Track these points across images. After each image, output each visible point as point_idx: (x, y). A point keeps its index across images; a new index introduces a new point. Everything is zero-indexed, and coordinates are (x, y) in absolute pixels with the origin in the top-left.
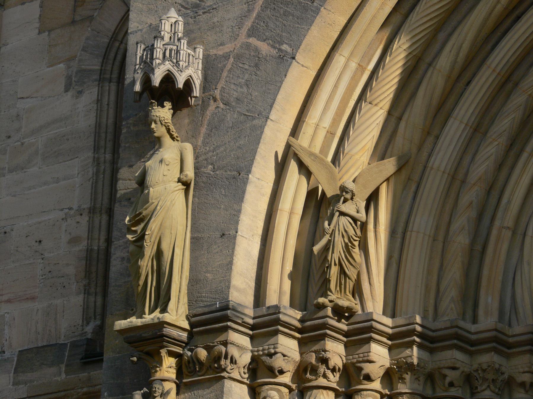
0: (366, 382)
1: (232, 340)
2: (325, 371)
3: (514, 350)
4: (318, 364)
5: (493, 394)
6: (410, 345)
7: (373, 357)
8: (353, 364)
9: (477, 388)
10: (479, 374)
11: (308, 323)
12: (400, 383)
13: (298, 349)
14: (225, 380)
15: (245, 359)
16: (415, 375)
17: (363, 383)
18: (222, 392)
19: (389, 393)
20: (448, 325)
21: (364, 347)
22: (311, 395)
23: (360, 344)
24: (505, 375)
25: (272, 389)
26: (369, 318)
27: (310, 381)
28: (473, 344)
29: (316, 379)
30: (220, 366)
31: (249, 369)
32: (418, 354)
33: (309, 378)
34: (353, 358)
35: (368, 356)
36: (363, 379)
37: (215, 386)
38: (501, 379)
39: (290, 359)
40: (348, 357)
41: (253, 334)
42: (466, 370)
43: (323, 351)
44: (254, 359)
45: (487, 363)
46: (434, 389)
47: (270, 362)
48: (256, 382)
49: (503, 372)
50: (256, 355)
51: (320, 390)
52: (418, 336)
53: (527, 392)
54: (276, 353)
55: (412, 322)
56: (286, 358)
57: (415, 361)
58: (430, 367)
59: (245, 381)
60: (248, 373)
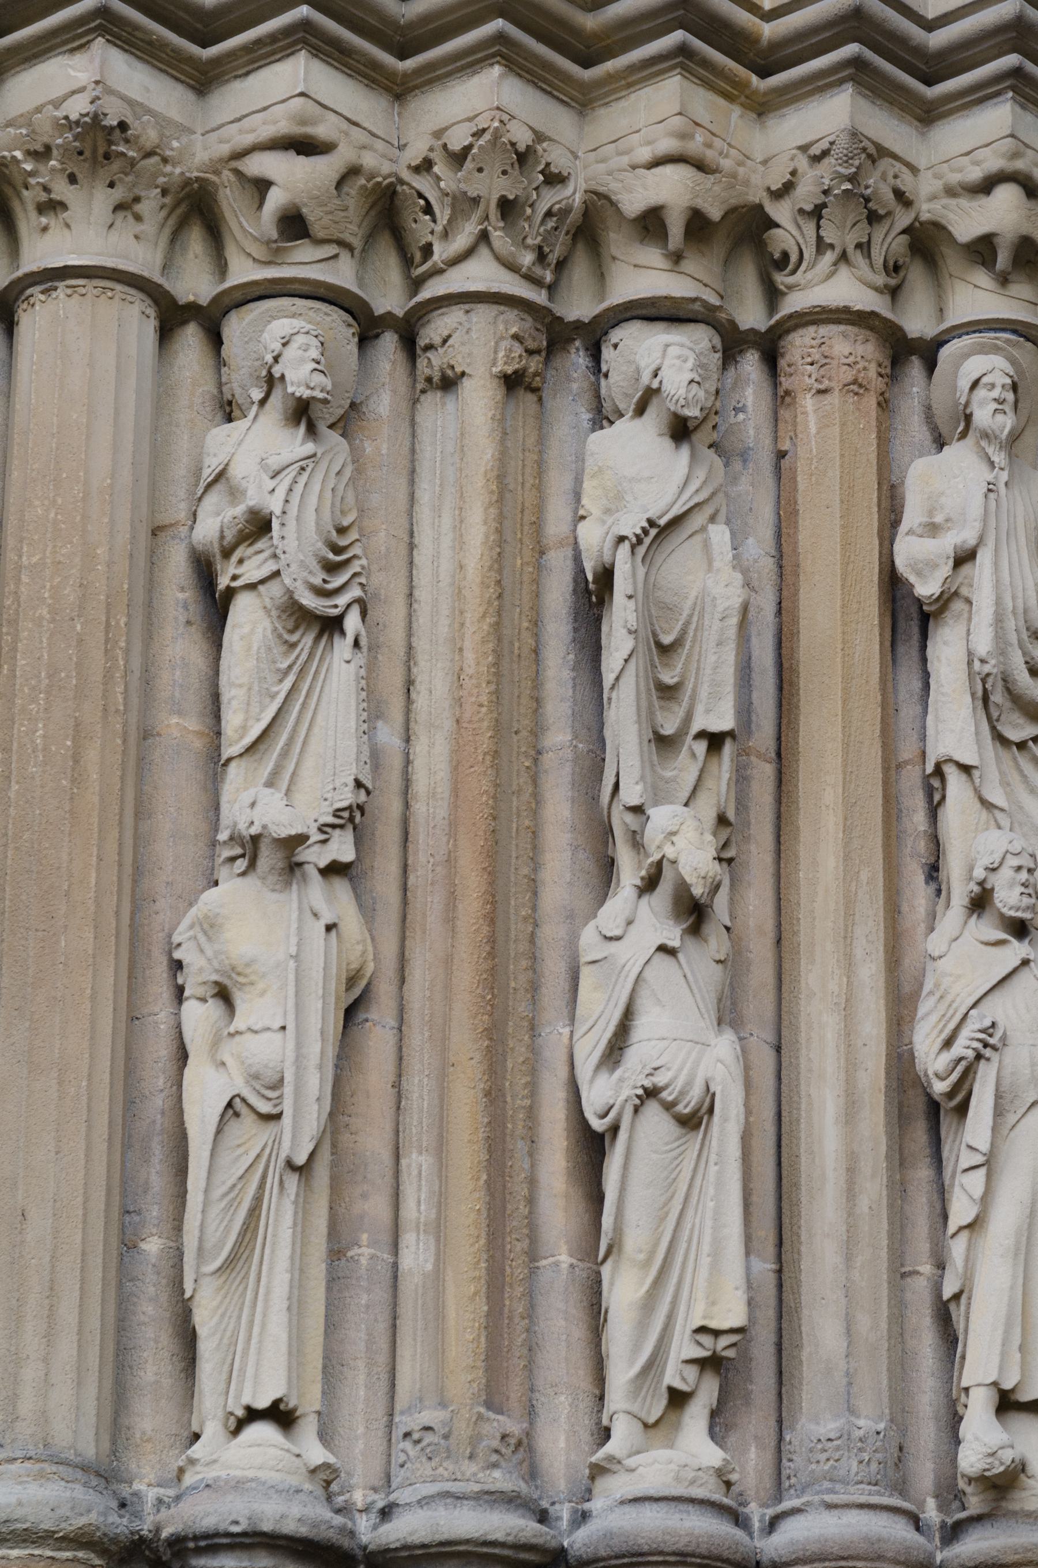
9: (427, 250)
16: (111, 185)
24: (569, 191)
38: (542, 208)
42: (368, 161)
45: (470, 119)
46: (222, 268)
49: (554, 169)
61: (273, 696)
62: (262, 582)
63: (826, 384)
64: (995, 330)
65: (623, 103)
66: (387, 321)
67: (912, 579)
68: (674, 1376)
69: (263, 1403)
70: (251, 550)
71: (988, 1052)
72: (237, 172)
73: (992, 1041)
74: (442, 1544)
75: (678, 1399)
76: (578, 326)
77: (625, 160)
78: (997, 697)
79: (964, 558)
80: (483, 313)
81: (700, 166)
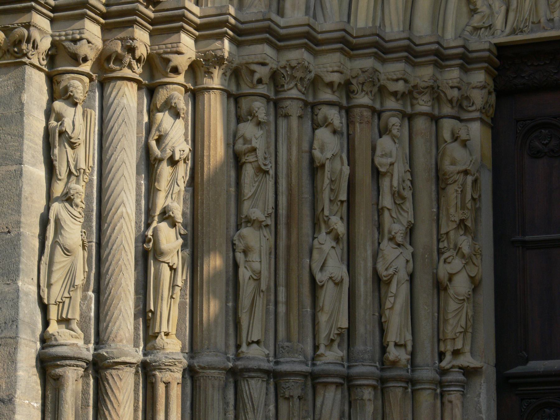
0: (172, 75)
1: (35, 22)
2: (130, 61)
3: (324, 48)
4: (124, 53)
5: (299, 93)
6: (220, 37)
7: (182, 48)
8: (159, 54)
9: (283, 86)
10: (287, 71)
11: (114, 8)
12: (206, 77)
13: (100, 36)
14: (26, 66)
15: (45, 44)
17: (169, 76)
18: (23, 80)
19: (192, 88)
20: (260, 17)
21: (173, 37)
22: (115, 86)
23: (168, 34)
25: (73, 79)
26: (181, 6)
27: (113, 71)
28: (281, 38)
29: (121, 70)
30: (21, 50)
31: (47, 55)
32: (230, 48)
33: (112, 68)
34: (159, 49)
35: (178, 47)
36: (170, 72)
37: (13, 72)
39: (93, 46)
40: (153, 47)
41: (54, 16)
43: (130, 39)
44: (54, 44)
45: (296, 60)
47: (74, 48)
48: (56, 69)
50: (57, 41)
51: (125, 82)
52: (231, 29)
53: (334, 92)
54: (81, 39)
55: (224, 12)
56: (90, 44)
57: (226, 55)
58: (237, 61)
59: (43, 67)
60: (46, 59)
61: (253, 186)
62: (253, 162)
63: (362, 121)
64: (396, 111)
65: (325, 56)
66: (272, 99)
67: (379, 167)
68: (332, 337)
69: (255, 340)
70: (250, 154)
71: (396, 273)
72: (247, 67)
73: (397, 271)
74: (293, 372)
75: (332, 341)
76: (310, 103)
77: (325, 69)
78: (396, 195)
79: (392, 164)
80: (295, 102)
81: (341, 73)
